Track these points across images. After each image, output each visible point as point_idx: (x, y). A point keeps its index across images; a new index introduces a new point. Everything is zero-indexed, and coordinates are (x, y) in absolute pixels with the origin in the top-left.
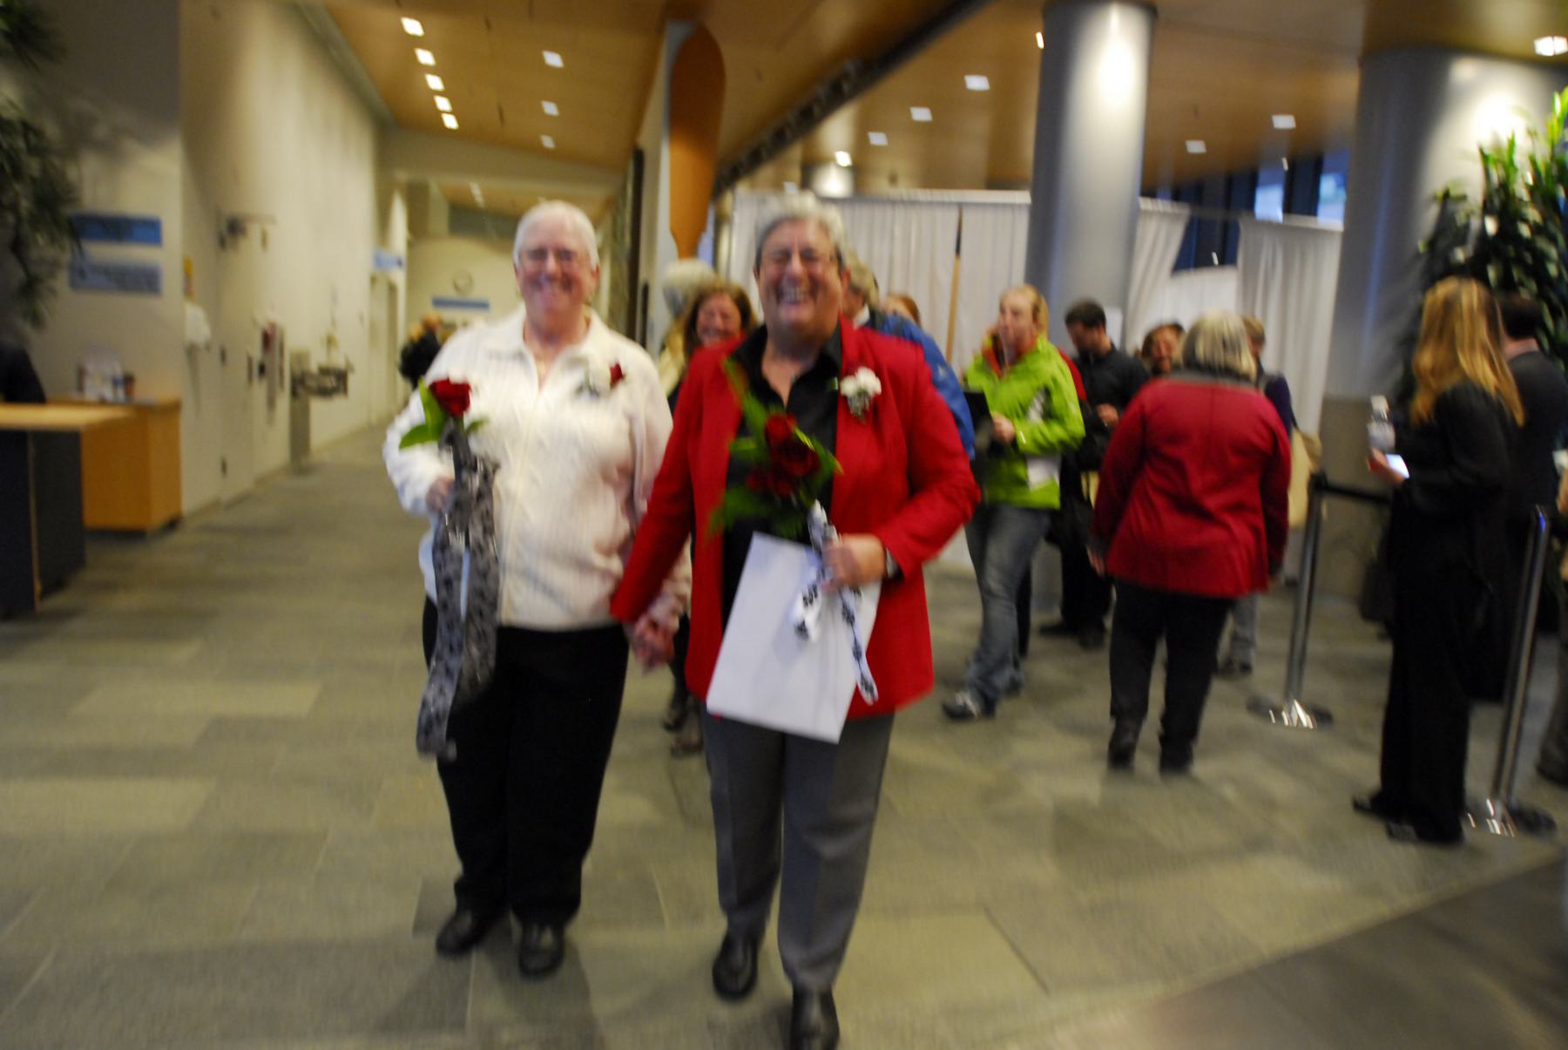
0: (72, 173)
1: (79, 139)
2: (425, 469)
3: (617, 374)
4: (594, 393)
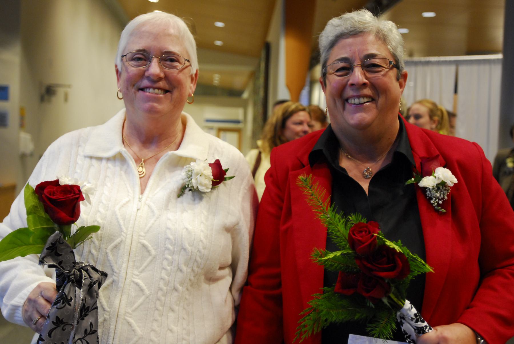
3: (219, 174)
4: (198, 194)
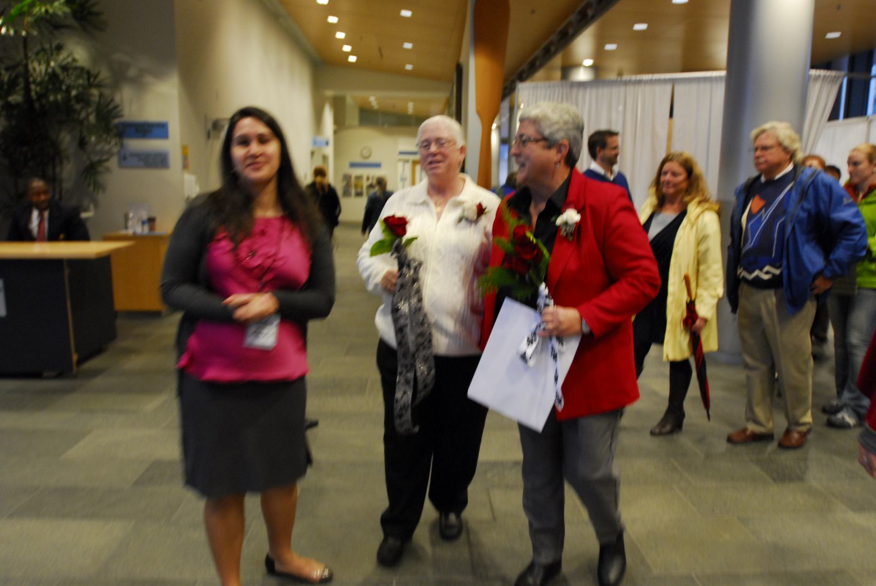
0: (117, 99)
1: (120, 77)
2: (378, 267)
3: (481, 210)
